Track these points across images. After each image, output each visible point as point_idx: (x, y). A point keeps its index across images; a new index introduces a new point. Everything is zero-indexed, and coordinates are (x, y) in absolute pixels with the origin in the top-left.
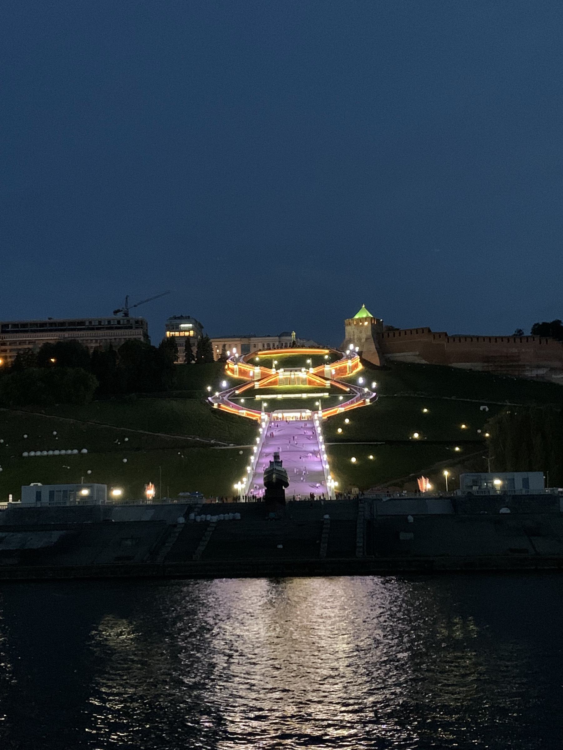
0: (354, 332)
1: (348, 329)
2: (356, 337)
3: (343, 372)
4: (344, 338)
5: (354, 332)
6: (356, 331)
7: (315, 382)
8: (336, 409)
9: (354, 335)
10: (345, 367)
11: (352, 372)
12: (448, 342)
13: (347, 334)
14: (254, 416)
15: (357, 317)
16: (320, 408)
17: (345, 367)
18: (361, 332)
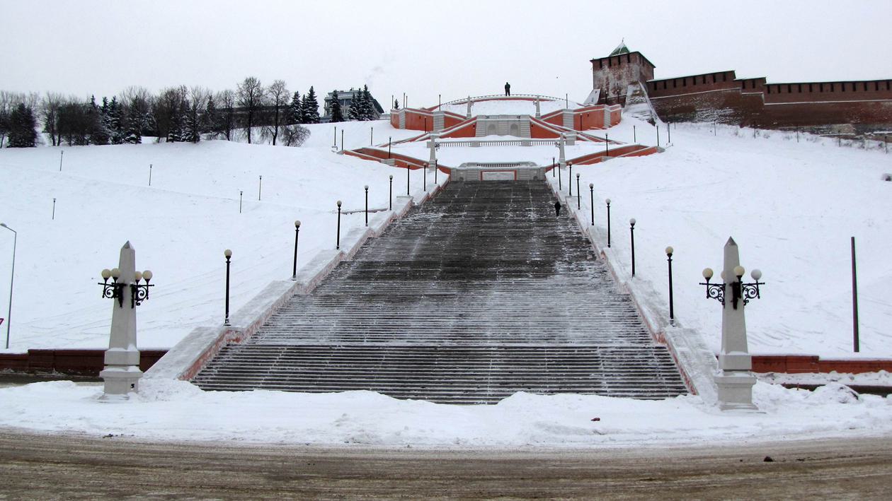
0: (607, 79)
2: (611, 86)
5: (607, 79)
6: (611, 76)
9: (608, 84)
12: (769, 92)
18: (620, 78)
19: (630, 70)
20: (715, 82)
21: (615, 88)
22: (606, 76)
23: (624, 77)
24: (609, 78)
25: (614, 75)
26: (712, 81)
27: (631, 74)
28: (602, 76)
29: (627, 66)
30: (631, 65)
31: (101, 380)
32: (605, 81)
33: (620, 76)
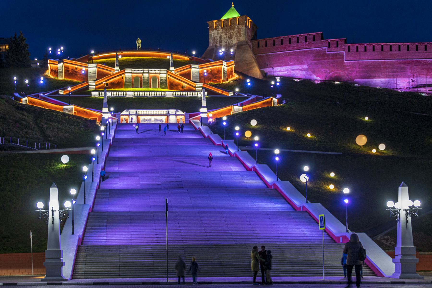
0: (220, 37)
1: (213, 33)
3: (215, 78)
4: (208, 45)
5: (220, 37)
6: (224, 36)
7: (179, 84)
8: (229, 108)
9: (221, 42)
10: (219, 71)
11: (227, 80)
12: (349, 51)
13: (211, 41)
14: (91, 115)
15: (224, 18)
16: (204, 103)
17: (219, 71)
18: (231, 37)
19: (239, 31)
20: (306, 41)
21: (226, 45)
22: (219, 35)
23: (234, 36)
24: (222, 37)
25: (226, 34)
26: (304, 41)
27: (240, 34)
28: (216, 35)
29: (237, 27)
30: (240, 27)
31: (43, 267)
32: (219, 39)
33: (231, 35)
